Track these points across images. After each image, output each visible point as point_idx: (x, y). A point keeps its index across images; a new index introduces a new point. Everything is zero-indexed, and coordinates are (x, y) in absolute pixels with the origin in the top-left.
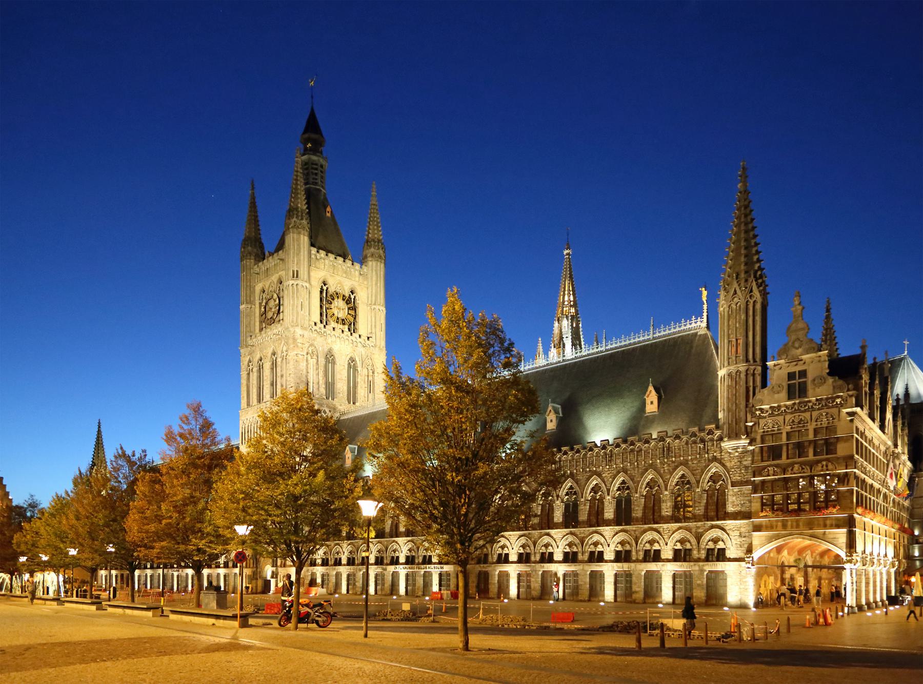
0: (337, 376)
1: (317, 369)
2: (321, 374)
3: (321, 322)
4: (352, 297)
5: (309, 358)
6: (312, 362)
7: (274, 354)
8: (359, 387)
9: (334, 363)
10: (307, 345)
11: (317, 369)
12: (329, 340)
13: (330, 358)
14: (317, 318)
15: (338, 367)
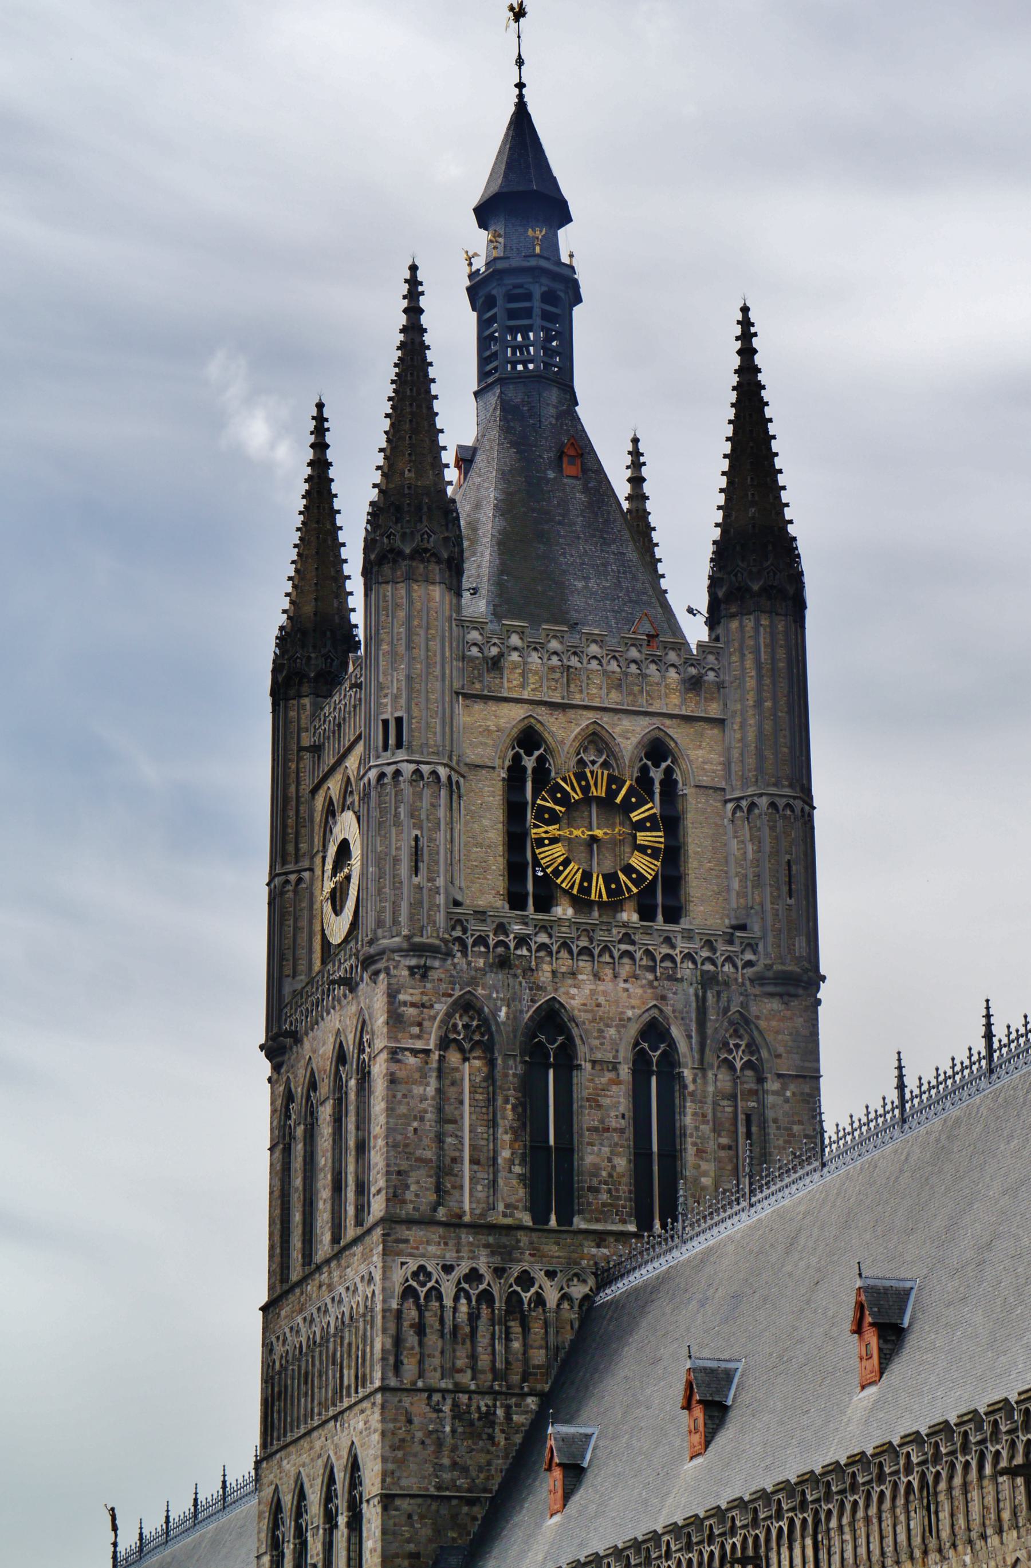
0: (587, 1118)
1: (491, 1100)
2: (508, 1115)
3: (516, 901)
4: (657, 775)
5: (454, 1057)
6: (469, 1071)
7: (341, 1057)
8: (691, 1150)
9: (567, 1063)
10: (441, 1008)
11: (491, 1100)
12: (544, 975)
13: (551, 1038)
14: (486, 889)
15: (586, 1080)
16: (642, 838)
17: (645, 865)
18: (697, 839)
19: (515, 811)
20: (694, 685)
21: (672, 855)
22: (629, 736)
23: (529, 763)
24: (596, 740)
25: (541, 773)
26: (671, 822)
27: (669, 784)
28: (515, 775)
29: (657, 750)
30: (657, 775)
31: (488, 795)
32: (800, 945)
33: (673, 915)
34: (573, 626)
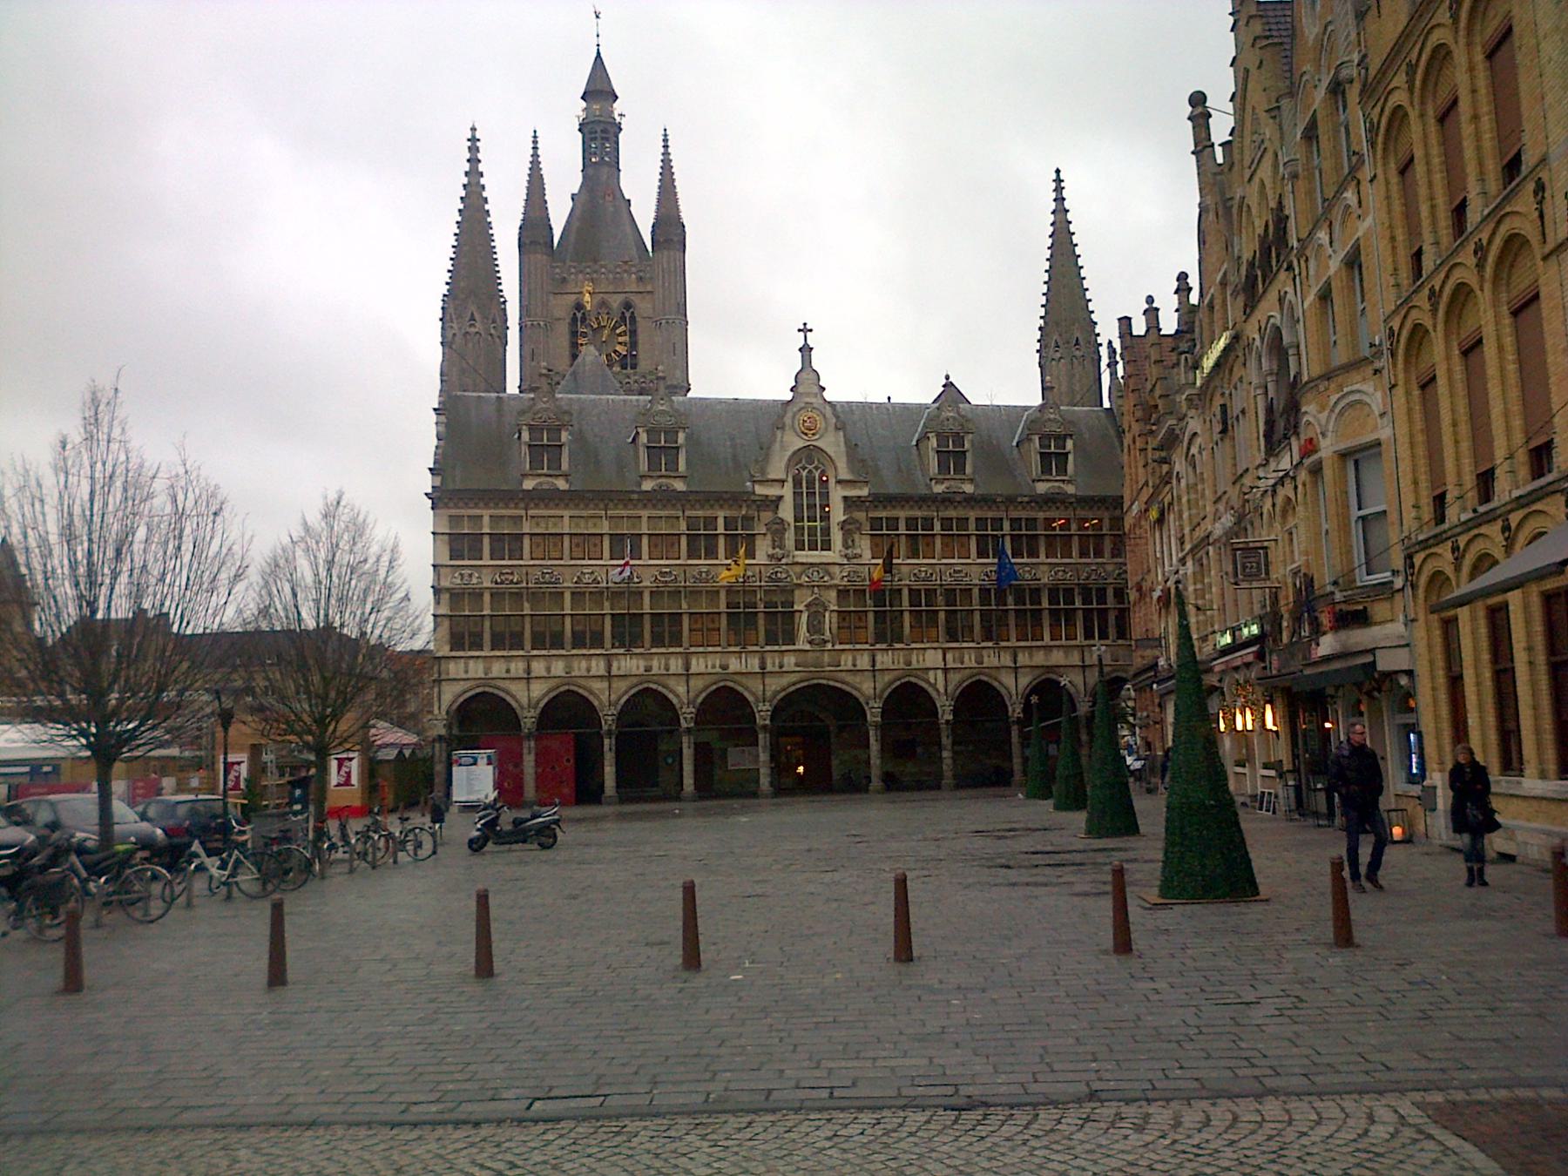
4: (628, 315)
16: (621, 339)
17: (622, 350)
18: (642, 337)
19: (574, 334)
20: (640, 279)
21: (634, 345)
22: (616, 302)
23: (579, 315)
24: (603, 304)
25: (584, 319)
26: (633, 333)
27: (633, 318)
28: (574, 319)
29: (628, 306)
30: (628, 315)
31: (563, 329)
32: (678, 373)
33: (634, 367)
34: (595, 261)
